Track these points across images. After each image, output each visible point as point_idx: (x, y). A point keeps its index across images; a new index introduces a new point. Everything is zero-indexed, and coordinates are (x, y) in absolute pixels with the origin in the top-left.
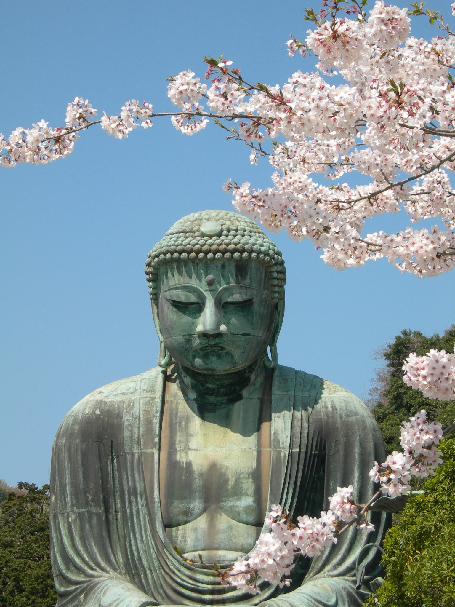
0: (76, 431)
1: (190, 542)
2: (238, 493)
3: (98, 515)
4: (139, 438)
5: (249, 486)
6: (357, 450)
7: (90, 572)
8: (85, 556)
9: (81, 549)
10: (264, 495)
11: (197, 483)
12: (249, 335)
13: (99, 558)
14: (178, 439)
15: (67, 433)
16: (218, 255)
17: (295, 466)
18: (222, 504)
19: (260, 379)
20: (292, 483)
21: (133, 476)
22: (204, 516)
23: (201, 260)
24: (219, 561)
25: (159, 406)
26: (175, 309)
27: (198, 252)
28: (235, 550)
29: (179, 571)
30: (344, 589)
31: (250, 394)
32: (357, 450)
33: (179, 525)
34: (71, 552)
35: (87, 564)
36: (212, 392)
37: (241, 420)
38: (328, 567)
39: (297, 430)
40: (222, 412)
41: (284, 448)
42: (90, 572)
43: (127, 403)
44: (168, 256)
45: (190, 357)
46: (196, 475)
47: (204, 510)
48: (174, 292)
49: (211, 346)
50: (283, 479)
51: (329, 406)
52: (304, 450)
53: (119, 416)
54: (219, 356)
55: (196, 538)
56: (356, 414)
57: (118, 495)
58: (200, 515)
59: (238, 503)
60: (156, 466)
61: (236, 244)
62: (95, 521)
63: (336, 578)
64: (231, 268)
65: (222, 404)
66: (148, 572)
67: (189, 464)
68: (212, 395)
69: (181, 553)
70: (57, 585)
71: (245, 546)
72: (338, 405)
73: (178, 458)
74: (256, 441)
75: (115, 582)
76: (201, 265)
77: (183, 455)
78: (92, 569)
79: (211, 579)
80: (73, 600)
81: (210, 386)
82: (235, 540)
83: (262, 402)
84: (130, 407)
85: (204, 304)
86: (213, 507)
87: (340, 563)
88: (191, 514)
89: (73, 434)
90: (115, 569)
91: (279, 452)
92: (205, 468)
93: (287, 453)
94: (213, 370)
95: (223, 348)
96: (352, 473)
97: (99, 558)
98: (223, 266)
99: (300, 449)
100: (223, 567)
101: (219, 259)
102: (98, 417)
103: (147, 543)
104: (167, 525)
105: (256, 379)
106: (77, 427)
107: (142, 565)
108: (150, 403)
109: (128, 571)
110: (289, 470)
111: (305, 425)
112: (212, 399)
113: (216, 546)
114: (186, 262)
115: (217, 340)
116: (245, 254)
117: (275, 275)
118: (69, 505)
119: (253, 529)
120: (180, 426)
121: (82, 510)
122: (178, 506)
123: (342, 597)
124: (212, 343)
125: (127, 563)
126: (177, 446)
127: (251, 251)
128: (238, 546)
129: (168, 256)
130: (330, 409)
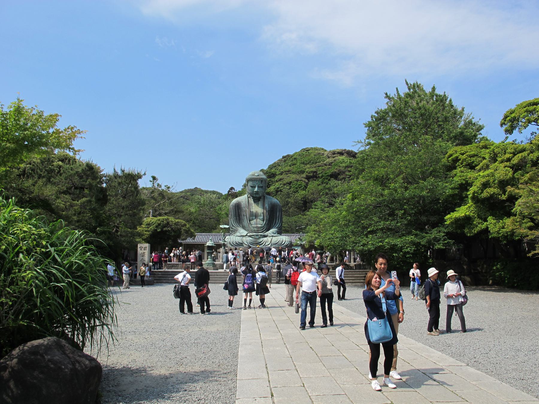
2: (260, 216)
5: (262, 215)
104: (250, 221)
122: (251, 218)
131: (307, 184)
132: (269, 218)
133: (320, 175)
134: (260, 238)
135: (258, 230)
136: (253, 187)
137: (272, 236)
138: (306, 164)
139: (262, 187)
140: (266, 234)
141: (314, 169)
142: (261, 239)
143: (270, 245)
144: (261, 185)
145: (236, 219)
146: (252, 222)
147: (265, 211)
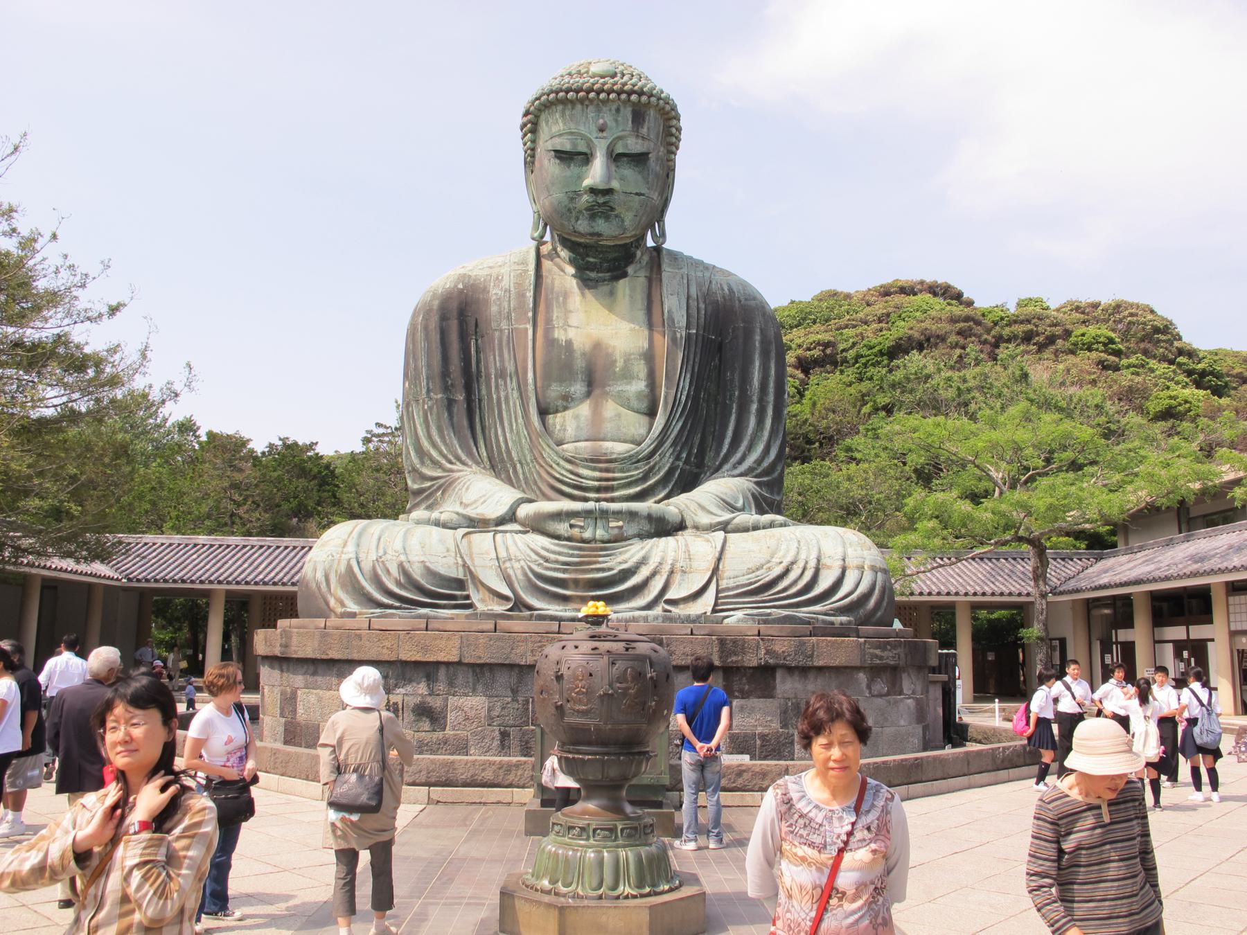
0: (435, 308)
1: (570, 432)
2: (627, 376)
4: (509, 313)
5: (641, 369)
6: (758, 338)
10: (657, 380)
11: (580, 364)
13: (460, 451)
14: (555, 315)
15: (424, 311)
16: (612, 96)
17: (693, 349)
18: (608, 389)
19: (646, 258)
20: (690, 368)
21: (501, 355)
23: (591, 101)
24: (606, 454)
25: (533, 278)
26: (557, 161)
27: (589, 91)
28: (625, 441)
32: (758, 338)
33: (557, 411)
34: (426, 444)
35: (445, 457)
36: (591, 267)
37: (627, 298)
38: (727, 467)
39: (694, 312)
40: (605, 288)
42: (449, 466)
43: (494, 275)
44: (552, 96)
45: (573, 220)
46: (578, 354)
49: (599, 205)
53: (485, 290)
54: (607, 218)
55: (578, 427)
56: (755, 299)
57: (483, 380)
58: (582, 400)
59: (628, 388)
61: (634, 86)
64: (627, 113)
66: (518, 466)
67: (569, 343)
68: (592, 270)
69: (560, 443)
70: (409, 482)
71: (638, 438)
73: (556, 336)
75: (479, 476)
76: (591, 108)
77: (562, 332)
78: (451, 463)
79: (597, 474)
80: (427, 497)
81: (591, 260)
83: (650, 280)
84: (498, 279)
86: (597, 392)
87: (740, 462)
88: (573, 399)
89: (430, 310)
90: (478, 464)
91: (675, 332)
92: (588, 348)
94: (599, 235)
95: (612, 209)
96: (752, 362)
98: (618, 110)
100: (610, 461)
101: (613, 101)
102: (461, 292)
103: (518, 432)
104: (543, 412)
105: (642, 257)
106: (436, 303)
107: (511, 459)
109: (493, 467)
111: (702, 306)
112: (593, 275)
113: (602, 436)
114: (571, 102)
115: (607, 197)
116: (644, 98)
118: (424, 391)
119: (644, 420)
120: (558, 302)
121: (440, 396)
122: (555, 390)
124: (601, 200)
125: (490, 459)
129: (552, 96)
131: (804, 383)
132: (694, 398)
133: (851, 354)
134: (620, 539)
135: (607, 474)
136: (573, 158)
137: (724, 527)
138: (791, 328)
141: (825, 337)
142: (632, 553)
143: (705, 604)
144: (634, 145)
145: (450, 404)
147: (662, 343)
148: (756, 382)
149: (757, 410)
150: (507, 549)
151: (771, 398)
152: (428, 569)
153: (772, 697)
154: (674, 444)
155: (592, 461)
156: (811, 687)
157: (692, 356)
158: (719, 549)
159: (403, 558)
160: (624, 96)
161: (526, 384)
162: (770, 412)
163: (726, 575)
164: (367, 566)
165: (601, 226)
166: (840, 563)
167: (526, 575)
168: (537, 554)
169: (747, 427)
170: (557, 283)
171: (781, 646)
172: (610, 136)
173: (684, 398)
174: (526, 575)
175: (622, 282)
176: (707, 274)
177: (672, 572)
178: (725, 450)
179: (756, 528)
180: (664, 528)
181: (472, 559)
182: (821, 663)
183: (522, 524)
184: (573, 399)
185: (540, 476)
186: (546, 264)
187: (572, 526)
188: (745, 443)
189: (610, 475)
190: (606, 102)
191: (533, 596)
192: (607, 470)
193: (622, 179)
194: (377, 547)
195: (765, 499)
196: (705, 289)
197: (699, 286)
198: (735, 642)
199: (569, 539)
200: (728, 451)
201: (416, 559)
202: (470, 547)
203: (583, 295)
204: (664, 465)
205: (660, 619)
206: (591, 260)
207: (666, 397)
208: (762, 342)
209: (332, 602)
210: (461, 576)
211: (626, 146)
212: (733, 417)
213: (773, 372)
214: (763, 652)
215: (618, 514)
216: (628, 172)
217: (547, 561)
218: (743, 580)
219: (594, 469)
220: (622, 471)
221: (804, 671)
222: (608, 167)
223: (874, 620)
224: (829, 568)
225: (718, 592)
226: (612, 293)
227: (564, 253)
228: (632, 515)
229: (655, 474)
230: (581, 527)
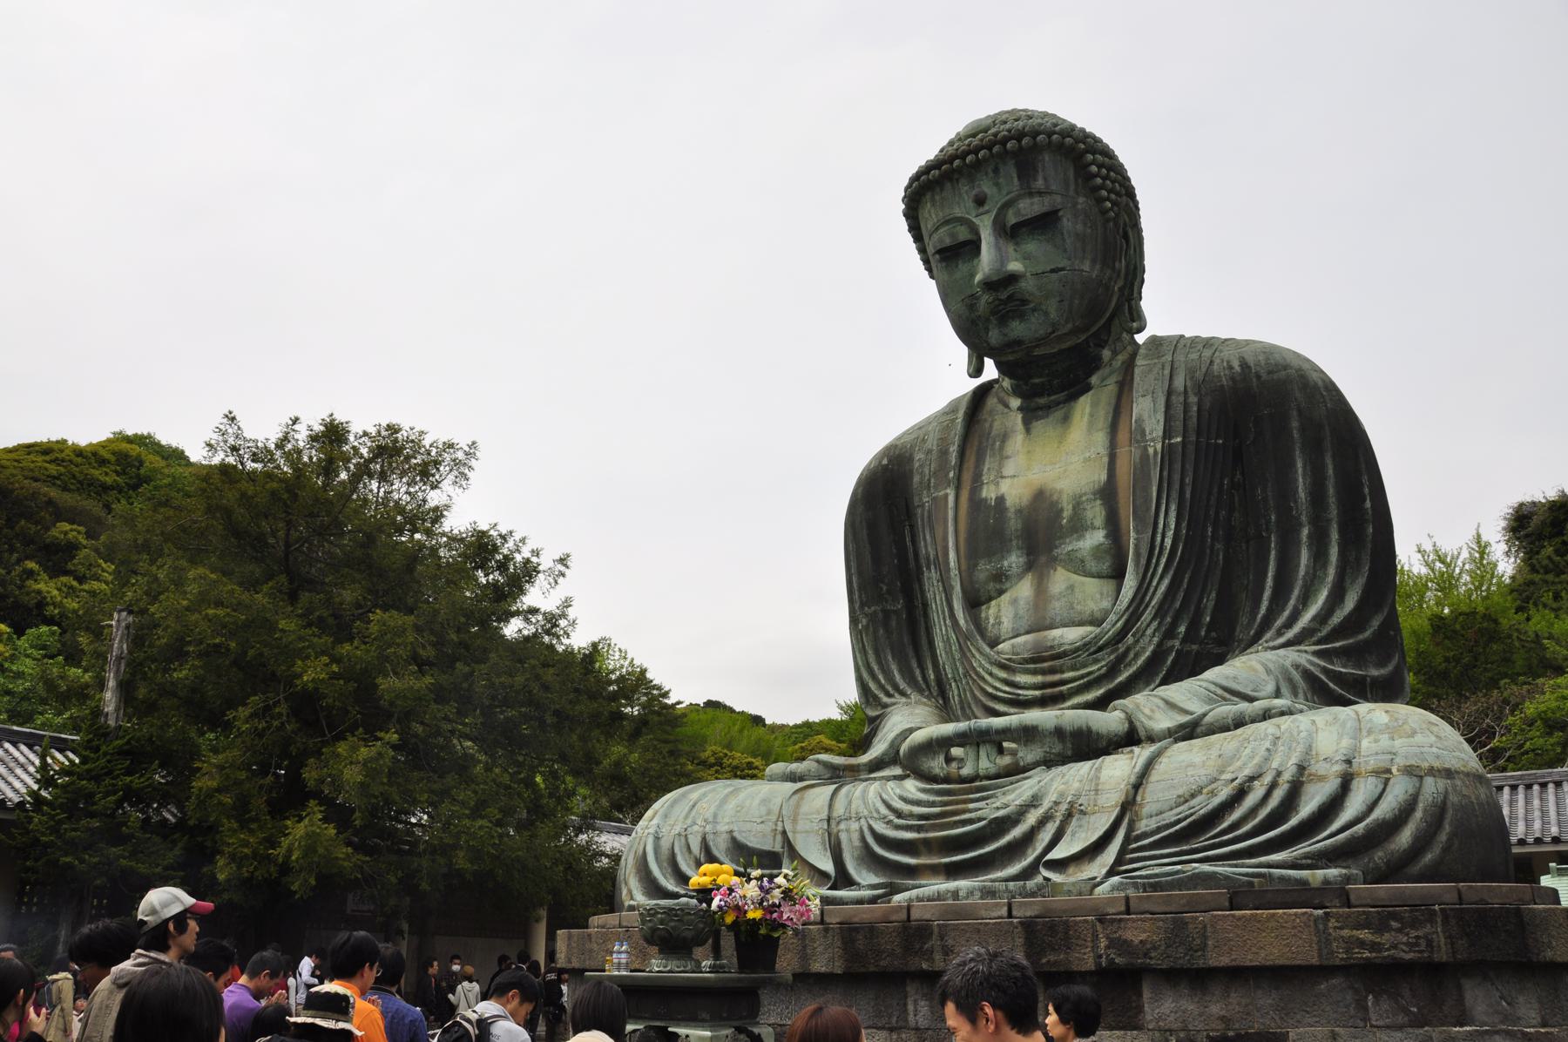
1: (1007, 624)
2: (1078, 527)
3: (895, 612)
5: (1096, 513)
6: (1295, 424)
7: (886, 700)
8: (881, 677)
9: (876, 668)
11: (1014, 524)
12: (1063, 269)
13: (898, 677)
17: (1178, 466)
20: (1175, 495)
22: (1029, 576)
23: (959, 170)
24: (1052, 647)
28: (1081, 624)
29: (991, 674)
30: (1297, 666)
31: (1103, 380)
32: (1295, 424)
33: (990, 599)
35: (882, 687)
38: (1268, 635)
39: (1178, 410)
40: (1059, 414)
41: (1153, 440)
42: (886, 700)
46: (1011, 514)
47: (1029, 567)
48: (936, 237)
50: (1155, 489)
51: (1236, 365)
52: (1193, 438)
53: (911, 459)
54: (1021, 316)
55: (1016, 615)
56: (1286, 367)
58: (1020, 577)
59: (1081, 544)
60: (951, 514)
62: (894, 623)
63: (1282, 652)
64: (1010, 169)
65: (1058, 404)
67: (1001, 500)
68: (1041, 395)
69: (993, 643)
71: (1098, 615)
72: (1251, 361)
73: (984, 494)
74: (1107, 443)
76: (963, 181)
77: (992, 487)
78: (889, 695)
79: (1039, 679)
81: (1037, 381)
82: (1079, 607)
85: (980, 240)
86: (1043, 559)
87: (1289, 624)
88: (1007, 577)
90: (920, 691)
91: (1145, 448)
92: (1025, 501)
93: (1159, 446)
94: (1018, 342)
95: (1024, 302)
96: (1293, 465)
97: (898, 677)
98: (996, 171)
99: (1184, 437)
101: (985, 160)
102: (885, 468)
108: (947, 429)
110: (1165, 473)
111: (1193, 399)
112: (1042, 401)
113: (1048, 622)
115: (1010, 290)
117: (1094, 169)
122: (984, 569)
123: (1290, 681)
124: (1004, 296)
126: (985, 479)
127: (1035, 133)
128: (1086, 617)
130: (1238, 369)
134: (1016, 771)
139: (1044, 223)
140: (1109, 721)
144: (1029, 207)
146: (1005, 612)
148: (1302, 494)
149: (1310, 536)
150: (850, 803)
151: (1333, 512)
152: (734, 840)
153: (1138, 1027)
154: (1160, 612)
155: (1033, 660)
156: (1216, 1009)
157: (1177, 477)
158: (1137, 769)
159: (708, 828)
160: (996, 149)
161: (948, 570)
162: (1335, 536)
163: (1145, 811)
164: (665, 844)
165: (1018, 329)
166: (1339, 768)
167: (863, 839)
168: (889, 806)
169: (1298, 565)
170: (997, 425)
171: (1136, 934)
172: (992, 207)
173: (1168, 542)
174: (863, 839)
175: (1082, 399)
176: (1207, 353)
177: (1069, 815)
178: (1263, 610)
179: (1239, 723)
180: (1086, 746)
181: (795, 821)
182: (1225, 961)
183: (904, 767)
184: (1007, 577)
185: (974, 696)
186: (992, 402)
187: (949, 760)
188: (1296, 592)
189: (1057, 677)
190: (978, 165)
191: (869, 870)
192: (1052, 671)
193: (1026, 257)
194: (686, 817)
195: (1337, 677)
196: (1199, 375)
197: (1191, 372)
198: (1052, 928)
199: (947, 780)
200: (1269, 609)
201: (726, 828)
202: (798, 806)
203: (1028, 430)
204: (1144, 649)
205: (978, 894)
206: (1037, 381)
207: (1137, 546)
208: (1303, 429)
209: (624, 892)
210: (778, 848)
211: (1018, 213)
212: (1273, 552)
213: (1331, 472)
214: (1103, 943)
215: (1006, 733)
216: (1031, 246)
217: (899, 814)
218: (1170, 817)
219: (1035, 672)
220: (1074, 668)
221: (1198, 978)
222: (998, 248)
223: (1416, 869)
224: (1322, 778)
225: (1128, 840)
226: (1066, 419)
227: (1007, 383)
228: (1028, 734)
229: (1129, 664)
230: (961, 760)
